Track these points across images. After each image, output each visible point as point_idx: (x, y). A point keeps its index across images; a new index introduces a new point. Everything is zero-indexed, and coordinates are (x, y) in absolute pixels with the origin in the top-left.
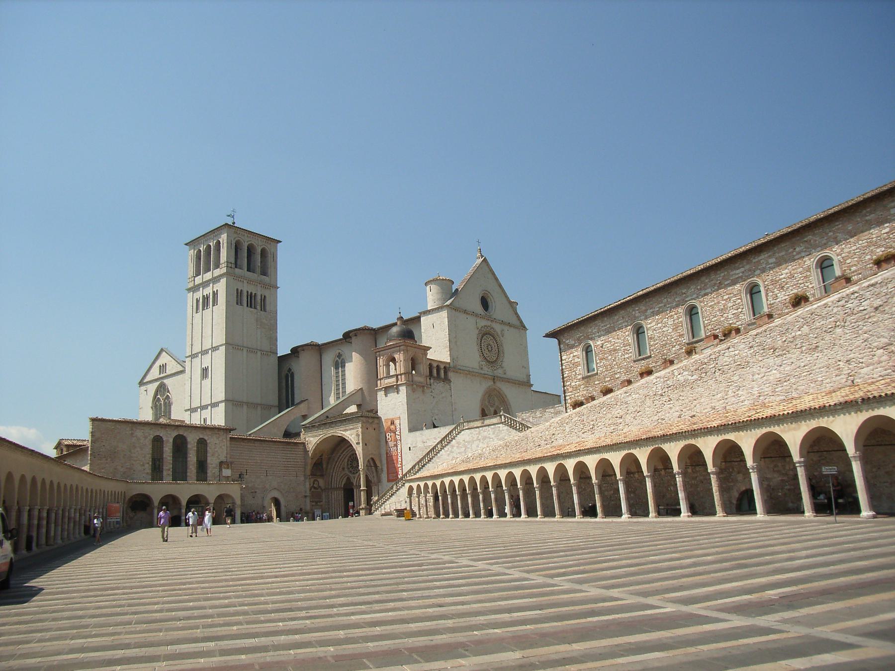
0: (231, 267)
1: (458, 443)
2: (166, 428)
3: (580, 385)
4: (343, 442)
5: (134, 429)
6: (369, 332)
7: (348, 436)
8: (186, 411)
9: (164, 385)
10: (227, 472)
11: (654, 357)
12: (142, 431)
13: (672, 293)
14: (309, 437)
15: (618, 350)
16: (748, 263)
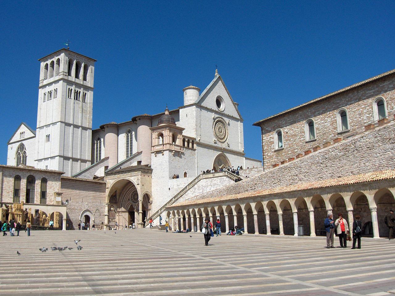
0: (66, 75)
2: (23, 171)
3: (273, 155)
4: (129, 183)
5: (4, 170)
7: (132, 180)
8: (35, 161)
9: (23, 145)
10: (59, 199)
11: (318, 140)
12: (9, 172)
13: (331, 103)
14: (109, 179)
15: (297, 135)
16: (377, 87)
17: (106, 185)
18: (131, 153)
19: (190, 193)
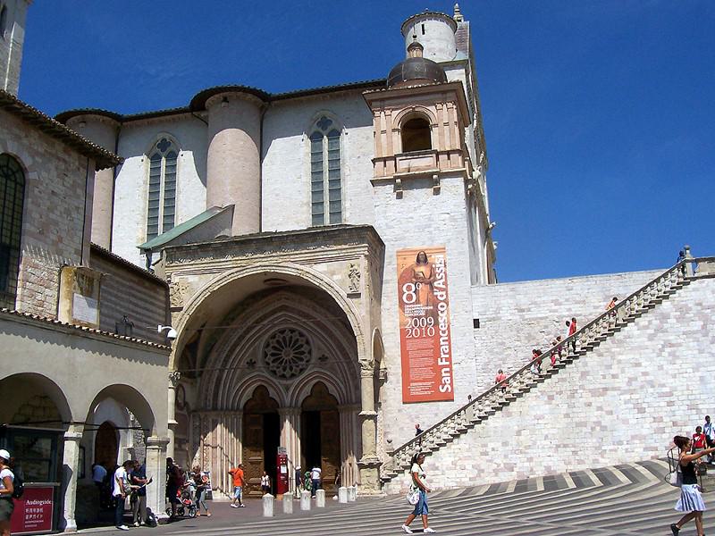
1: (680, 309)
6: (255, 98)
17: (167, 296)
18: (170, 216)
19: (637, 332)
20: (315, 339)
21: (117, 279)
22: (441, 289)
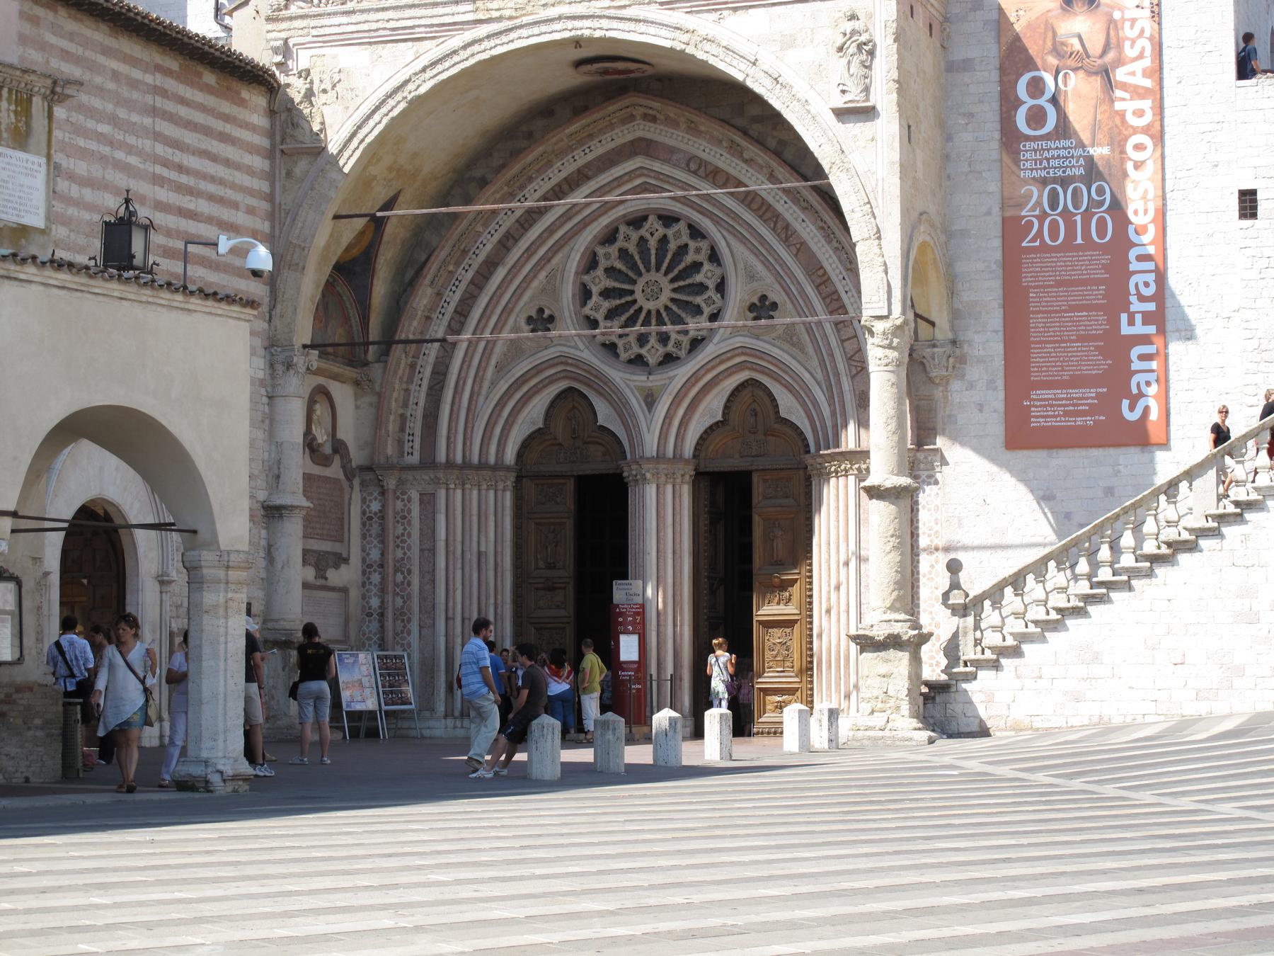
20: (738, 248)
21: (114, 64)
22: (1138, 93)
